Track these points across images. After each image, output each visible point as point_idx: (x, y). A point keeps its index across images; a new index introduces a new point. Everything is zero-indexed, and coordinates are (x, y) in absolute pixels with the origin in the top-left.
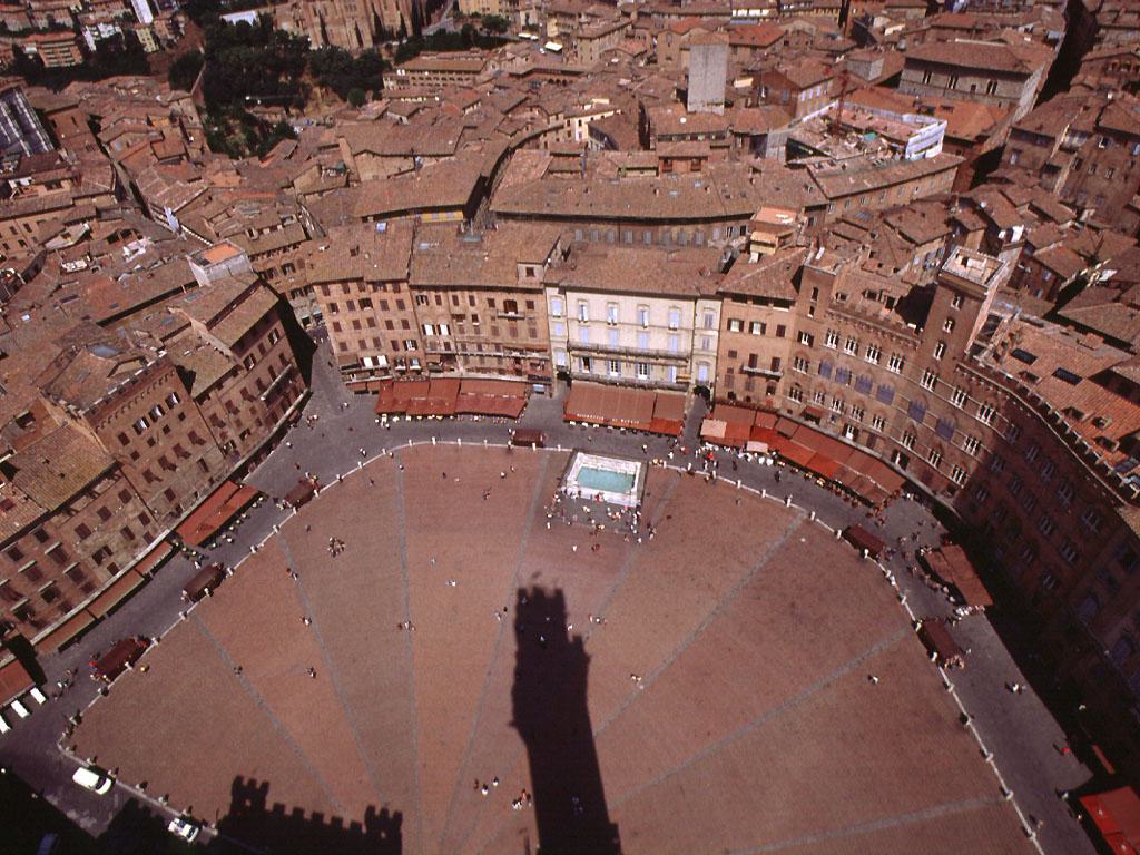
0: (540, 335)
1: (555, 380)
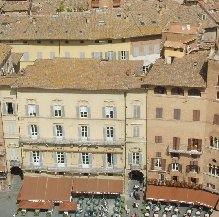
1: (9, 174)
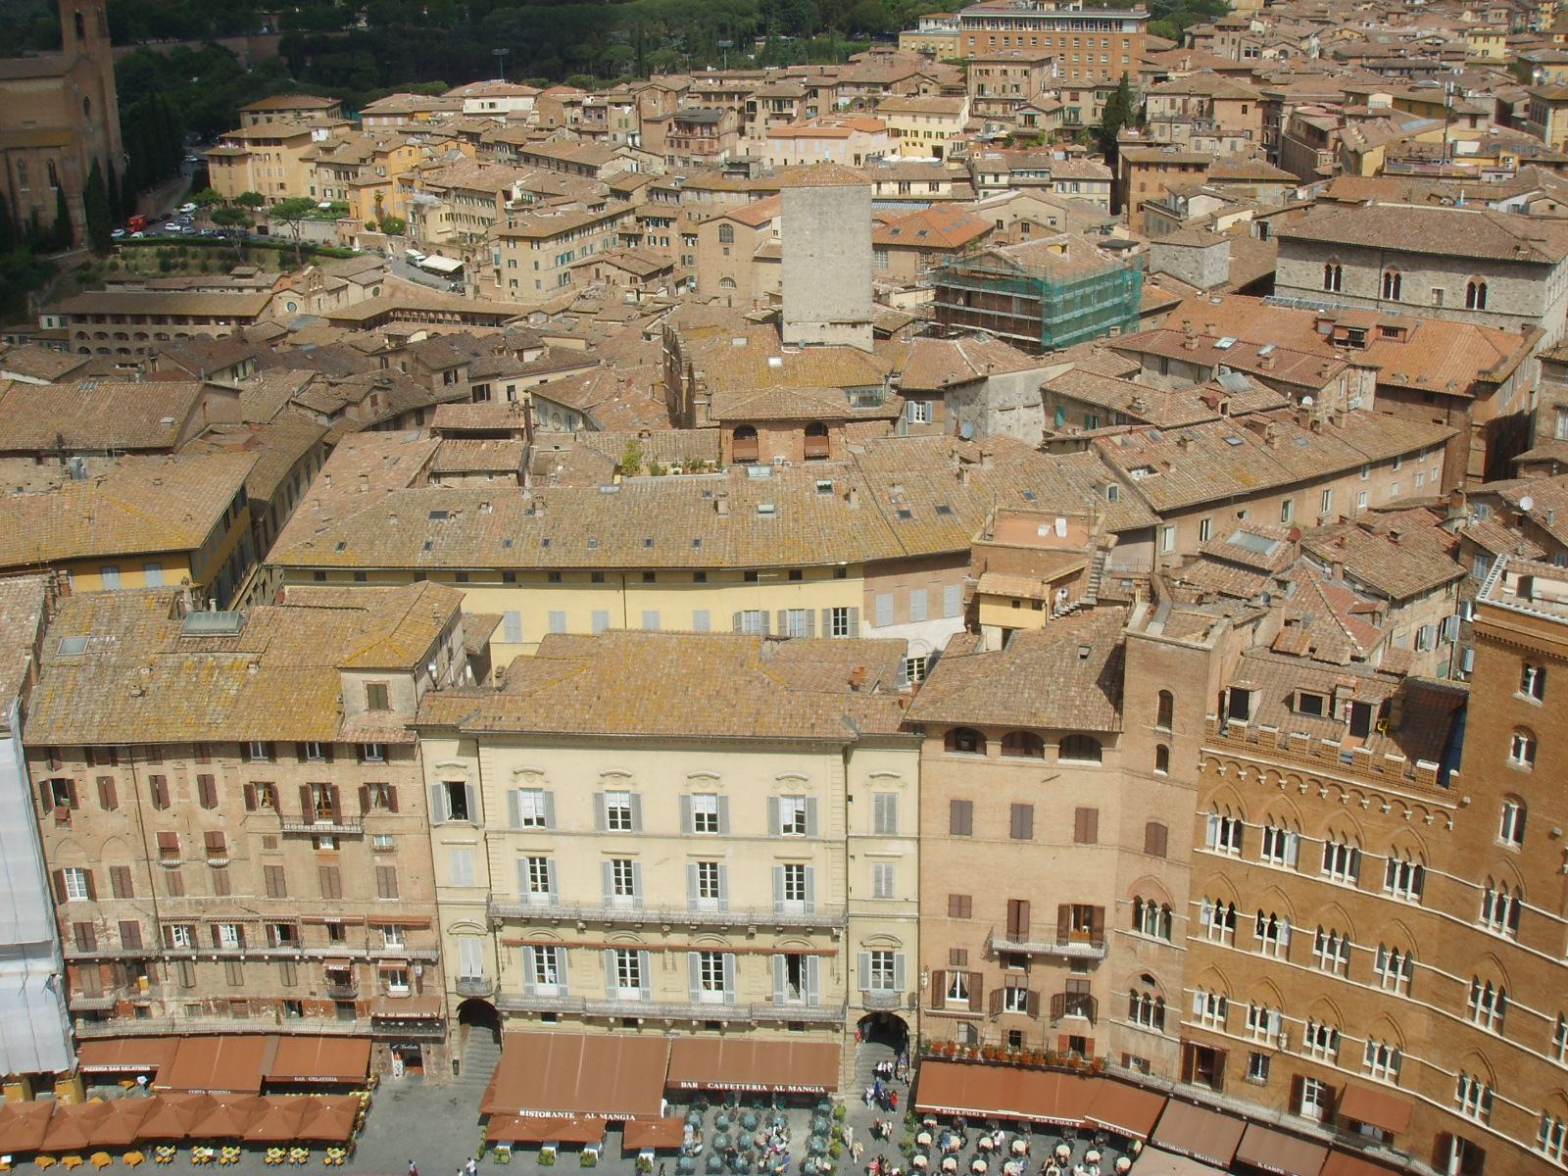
0: (409, 887)
1: (454, 1025)
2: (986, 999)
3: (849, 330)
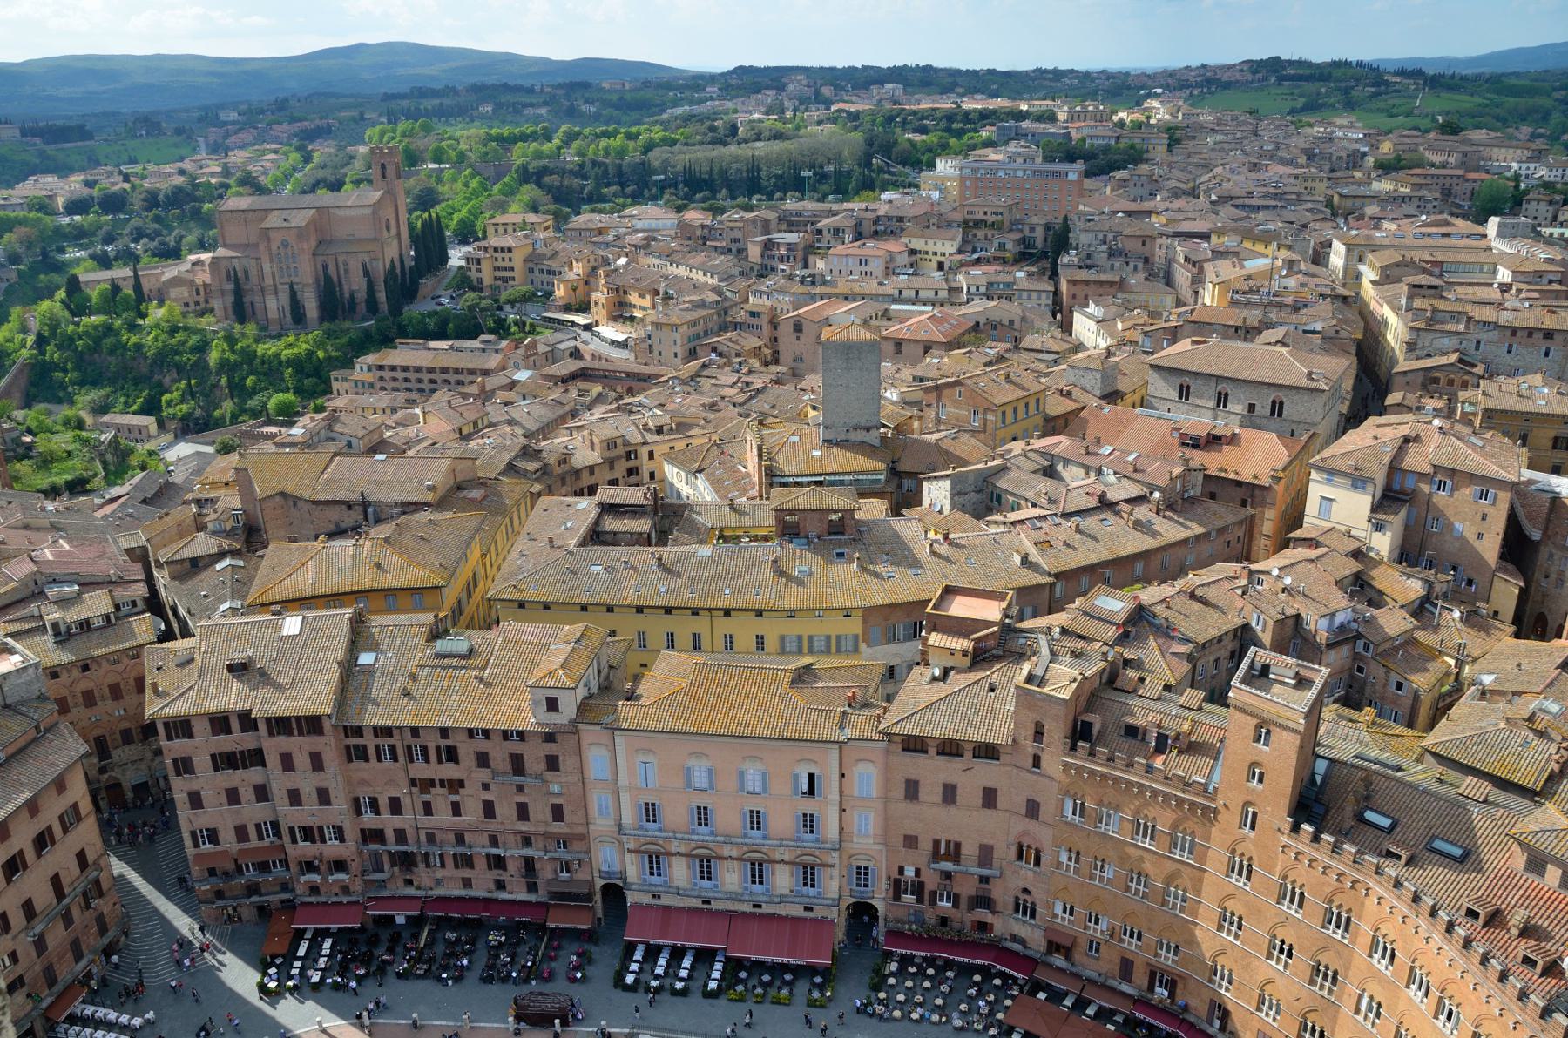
2: (927, 897)
3: (864, 433)
